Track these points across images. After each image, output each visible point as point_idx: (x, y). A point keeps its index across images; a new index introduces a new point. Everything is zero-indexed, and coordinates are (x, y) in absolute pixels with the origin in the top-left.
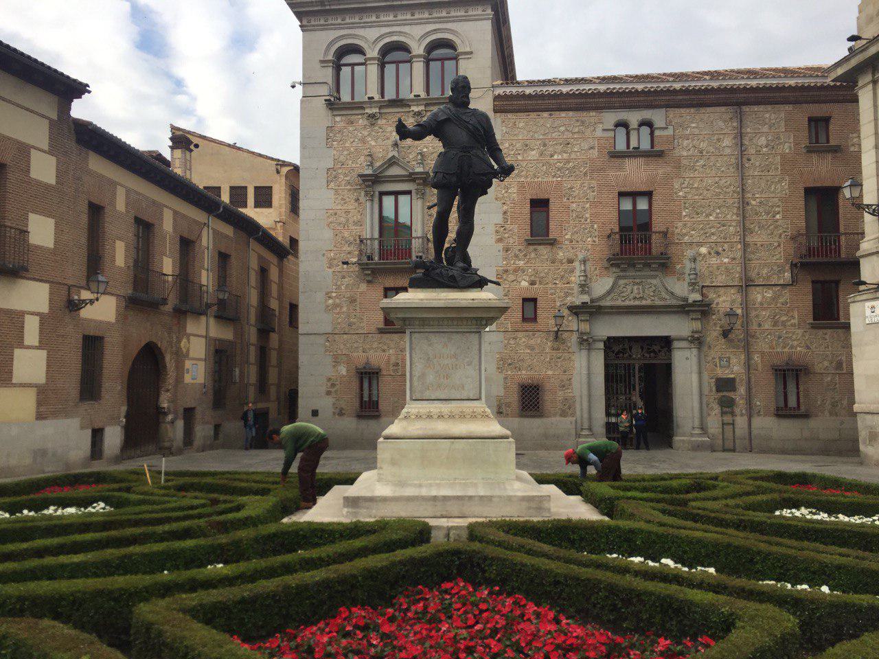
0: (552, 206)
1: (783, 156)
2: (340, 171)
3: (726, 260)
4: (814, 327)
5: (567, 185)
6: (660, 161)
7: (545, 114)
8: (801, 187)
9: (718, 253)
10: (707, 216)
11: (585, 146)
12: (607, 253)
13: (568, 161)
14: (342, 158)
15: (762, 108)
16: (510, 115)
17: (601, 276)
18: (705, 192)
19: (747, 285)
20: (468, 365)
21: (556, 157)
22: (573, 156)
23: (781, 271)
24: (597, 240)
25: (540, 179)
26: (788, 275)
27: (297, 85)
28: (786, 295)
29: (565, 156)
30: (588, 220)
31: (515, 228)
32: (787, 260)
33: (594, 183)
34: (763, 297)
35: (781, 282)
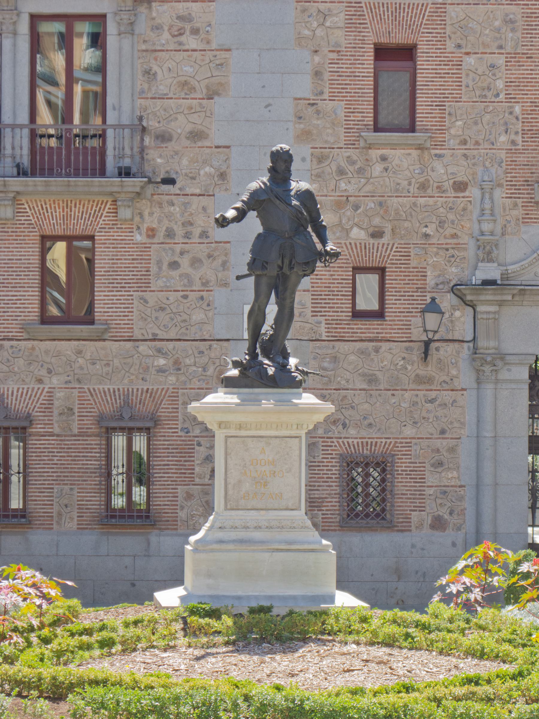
0: (424, 63)
20: (288, 472)
24: (519, 139)
30: (502, 96)
31: (340, 108)
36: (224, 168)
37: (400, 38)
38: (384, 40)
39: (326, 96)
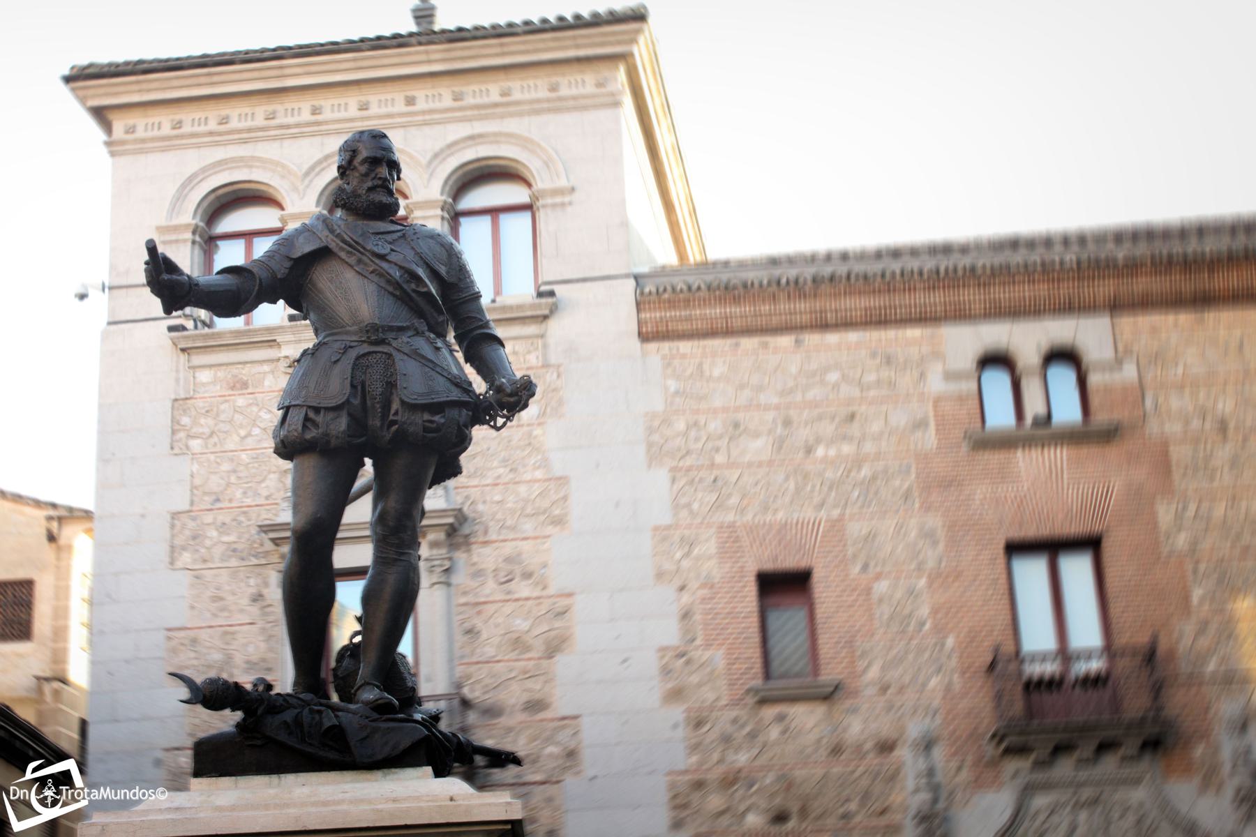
0: (821, 587)
2: (208, 518)
5: (856, 529)
6: (1113, 453)
7: (785, 341)
11: (900, 418)
12: (988, 722)
13: (858, 462)
14: (215, 483)
16: (685, 346)
17: (978, 784)
21: (820, 452)
22: (869, 447)
25: (780, 515)
27: (91, 292)
29: (847, 449)
33: (935, 521)
36: (572, 745)
37: (789, 562)
38: (769, 566)
39: (698, 642)
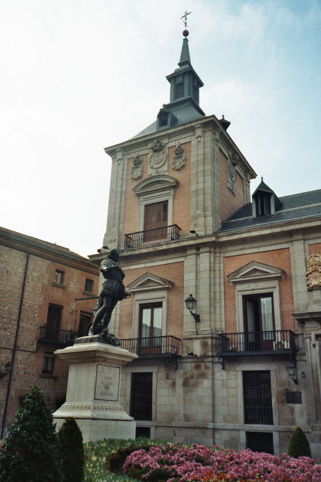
1: (43, 285)
3: (8, 334)
4: (42, 377)
8: (48, 302)
9: (5, 329)
10: (4, 307)
15: (38, 258)
18: (5, 294)
19: (15, 349)
23: (32, 345)
26: (35, 346)
28: (33, 357)
32: (36, 339)
34: (22, 357)
35: (32, 350)
